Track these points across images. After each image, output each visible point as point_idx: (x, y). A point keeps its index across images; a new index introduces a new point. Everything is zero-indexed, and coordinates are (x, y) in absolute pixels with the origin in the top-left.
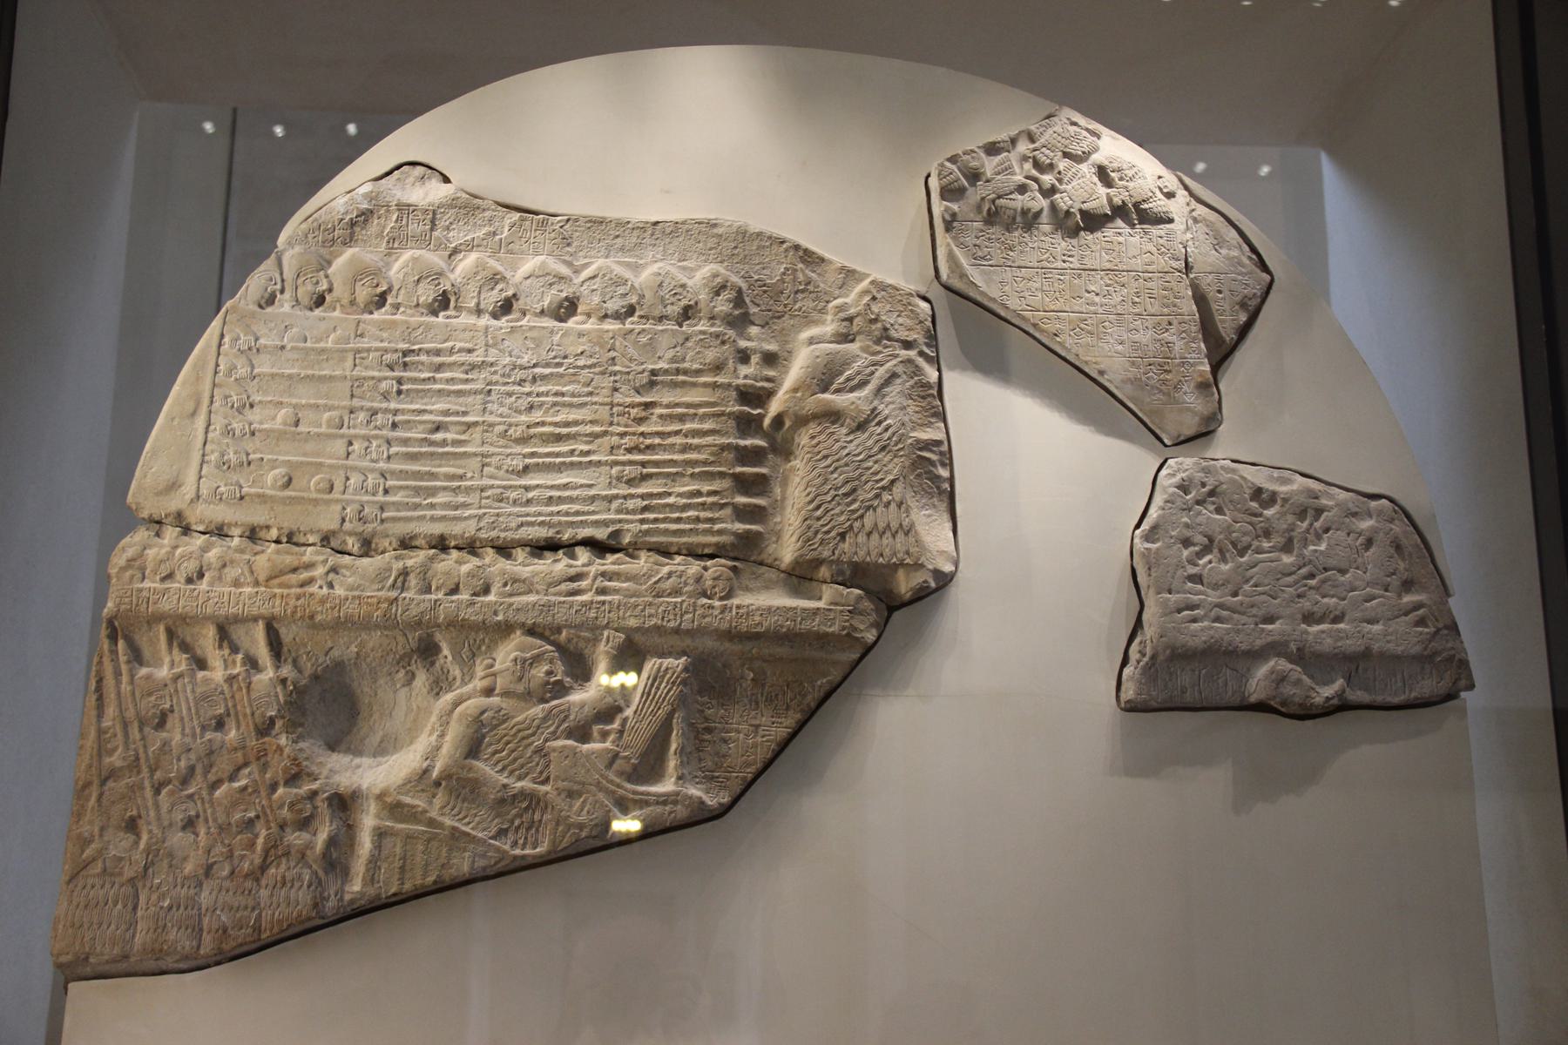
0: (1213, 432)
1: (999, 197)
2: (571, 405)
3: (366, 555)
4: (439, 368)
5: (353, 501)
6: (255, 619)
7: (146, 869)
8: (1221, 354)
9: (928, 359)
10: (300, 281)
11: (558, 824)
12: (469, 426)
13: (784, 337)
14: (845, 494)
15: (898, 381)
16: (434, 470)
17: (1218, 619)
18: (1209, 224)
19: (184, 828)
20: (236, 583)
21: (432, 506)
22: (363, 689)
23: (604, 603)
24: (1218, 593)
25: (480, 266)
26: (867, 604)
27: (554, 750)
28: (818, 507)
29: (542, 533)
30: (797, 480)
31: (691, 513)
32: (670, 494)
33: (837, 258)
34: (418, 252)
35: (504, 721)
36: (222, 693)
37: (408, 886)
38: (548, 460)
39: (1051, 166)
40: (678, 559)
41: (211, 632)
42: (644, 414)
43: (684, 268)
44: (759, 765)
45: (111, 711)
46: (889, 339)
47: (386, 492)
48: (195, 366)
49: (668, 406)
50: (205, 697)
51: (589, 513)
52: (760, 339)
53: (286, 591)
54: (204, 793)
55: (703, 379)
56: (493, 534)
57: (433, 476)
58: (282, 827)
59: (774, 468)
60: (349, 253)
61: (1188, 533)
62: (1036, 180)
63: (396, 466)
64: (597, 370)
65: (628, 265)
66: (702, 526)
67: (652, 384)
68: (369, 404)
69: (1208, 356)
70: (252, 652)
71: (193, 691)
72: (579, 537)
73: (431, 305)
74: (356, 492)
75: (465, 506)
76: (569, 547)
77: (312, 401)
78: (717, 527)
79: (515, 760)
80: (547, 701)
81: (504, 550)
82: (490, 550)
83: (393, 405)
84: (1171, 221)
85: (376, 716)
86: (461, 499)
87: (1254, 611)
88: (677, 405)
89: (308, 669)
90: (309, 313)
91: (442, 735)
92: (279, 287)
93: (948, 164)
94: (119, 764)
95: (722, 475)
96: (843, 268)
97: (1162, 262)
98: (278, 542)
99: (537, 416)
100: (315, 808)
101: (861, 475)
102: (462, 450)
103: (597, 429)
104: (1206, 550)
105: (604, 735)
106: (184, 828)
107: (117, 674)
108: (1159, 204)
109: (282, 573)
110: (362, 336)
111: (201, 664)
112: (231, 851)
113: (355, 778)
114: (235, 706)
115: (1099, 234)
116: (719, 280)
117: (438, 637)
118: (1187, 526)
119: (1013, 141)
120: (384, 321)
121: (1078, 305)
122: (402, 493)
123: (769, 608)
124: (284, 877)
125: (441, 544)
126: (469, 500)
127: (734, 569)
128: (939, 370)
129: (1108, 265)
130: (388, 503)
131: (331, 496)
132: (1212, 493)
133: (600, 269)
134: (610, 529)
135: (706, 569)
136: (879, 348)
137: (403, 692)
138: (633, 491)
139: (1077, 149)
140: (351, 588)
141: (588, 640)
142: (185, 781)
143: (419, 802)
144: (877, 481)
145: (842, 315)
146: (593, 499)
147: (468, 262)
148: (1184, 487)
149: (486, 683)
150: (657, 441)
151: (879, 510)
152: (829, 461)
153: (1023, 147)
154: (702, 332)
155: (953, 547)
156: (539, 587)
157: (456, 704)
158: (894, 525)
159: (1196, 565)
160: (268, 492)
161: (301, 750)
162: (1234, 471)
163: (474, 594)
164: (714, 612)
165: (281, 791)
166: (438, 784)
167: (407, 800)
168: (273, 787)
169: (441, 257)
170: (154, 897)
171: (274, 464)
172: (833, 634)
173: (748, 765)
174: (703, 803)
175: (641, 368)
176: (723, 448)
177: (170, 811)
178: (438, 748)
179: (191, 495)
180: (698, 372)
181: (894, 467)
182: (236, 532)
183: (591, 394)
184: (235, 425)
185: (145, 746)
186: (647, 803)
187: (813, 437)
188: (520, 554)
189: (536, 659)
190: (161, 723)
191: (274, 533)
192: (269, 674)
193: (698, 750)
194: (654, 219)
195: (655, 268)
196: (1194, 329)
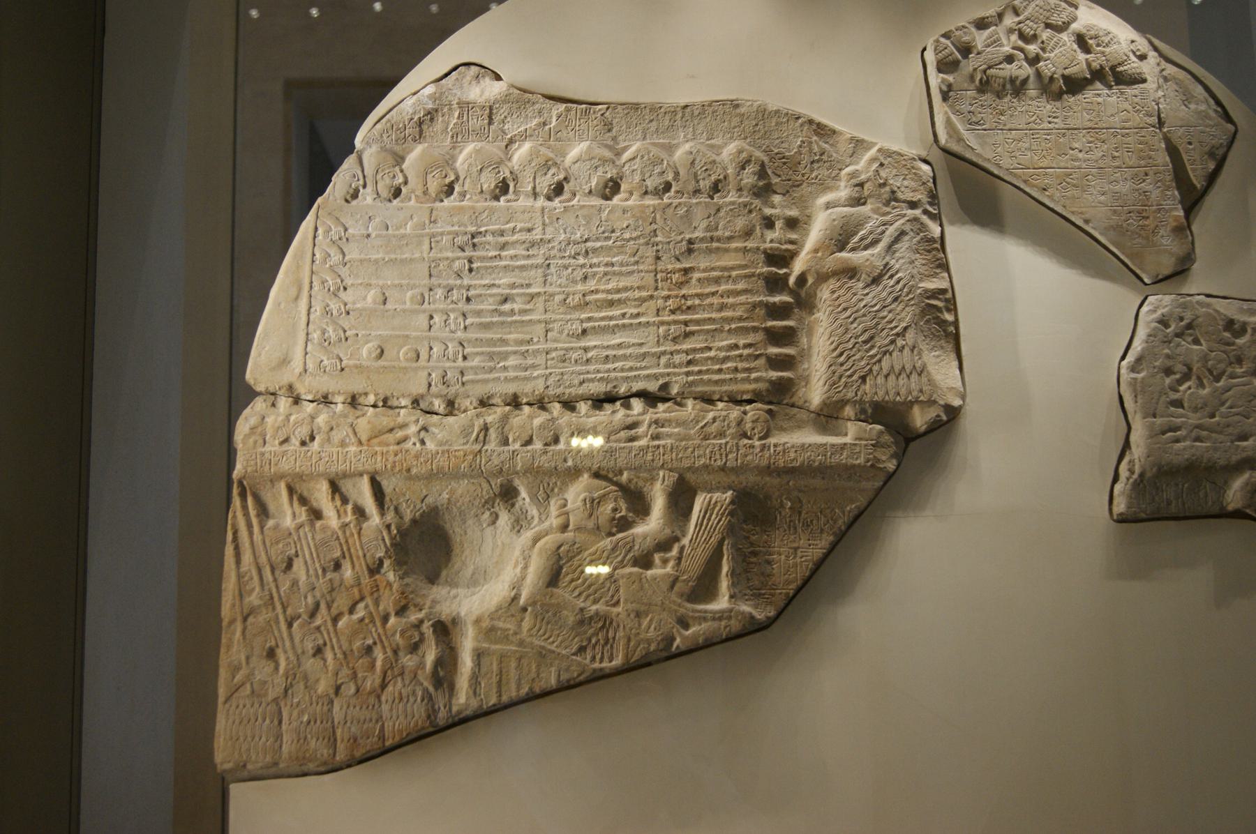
0: (1188, 269)
1: (990, 68)
2: (620, 274)
3: (450, 414)
4: (504, 246)
6: (361, 475)
7: (286, 691)
8: (1192, 200)
9: (932, 217)
10: (379, 177)
11: (629, 640)
13: (803, 203)
14: (864, 342)
15: (907, 238)
16: (505, 337)
17: (1198, 439)
18: (1178, 82)
19: (314, 655)
20: (343, 444)
21: (505, 368)
22: (455, 530)
23: (658, 447)
24: (1198, 415)
25: (534, 153)
26: (887, 438)
27: (623, 577)
28: (841, 354)
29: (598, 388)
30: (821, 330)
31: (729, 365)
32: (710, 349)
33: (846, 129)
34: (479, 145)
35: (579, 553)
36: (338, 538)
37: (505, 699)
38: (603, 323)
39: (1035, 37)
40: (720, 405)
41: (324, 487)
43: (712, 146)
44: (799, 582)
45: (247, 557)
46: (896, 200)
47: (465, 358)
48: (295, 256)
49: (705, 271)
50: (324, 543)
51: (641, 368)
52: (783, 207)
53: (385, 449)
54: (329, 623)
55: (734, 245)
56: (559, 391)
57: (504, 342)
58: (395, 652)
59: (800, 320)
60: (419, 149)
61: (1169, 363)
62: (1022, 50)
63: (472, 335)
64: (642, 241)
65: (662, 146)
66: (740, 376)
67: (690, 251)
68: (445, 283)
69: (1181, 202)
70: (360, 502)
71: (313, 538)
73: (493, 191)
74: (438, 360)
75: (534, 367)
76: (626, 400)
77: (396, 282)
78: (753, 375)
80: (614, 535)
81: (569, 405)
82: (557, 405)
83: (466, 282)
84: (1144, 81)
85: (467, 552)
86: (530, 361)
87: (1230, 430)
88: (713, 269)
89: (408, 516)
90: (389, 204)
91: (526, 567)
92: (361, 182)
93: (942, 40)
94: (257, 602)
95: (755, 329)
96: (852, 139)
97: (1137, 119)
98: (375, 406)
99: (592, 284)
100: (422, 634)
101: (877, 324)
102: (528, 318)
103: (644, 294)
104: (1186, 377)
105: (665, 562)
106: (314, 655)
107: (250, 526)
108: (1133, 65)
109: (381, 433)
110: (435, 222)
111: (316, 514)
114: (349, 549)
115: (1080, 97)
116: (744, 155)
117: (517, 482)
118: (1168, 357)
119: (1000, 16)
120: (454, 208)
121: (1063, 161)
122: (477, 359)
123: (803, 445)
124: (400, 694)
125: (515, 402)
127: (770, 412)
128: (941, 225)
129: (1090, 124)
130: (467, 368)
132: (1189, 326)
133: (638, 151)
134: (661, 382)
135: (745, 413)
136: (888, 209)
138: (678, 347)
139: (1057, 20)
140: (441, 444)
141: (646, 480)
142: (313, 614)
143: (510, 626)
144: (892, 329)
145: (854, 181)
146: (644, 355)
147: (522, 151)
148: (1163, 322)
149: (560, 521)
150: (697, 302)
151: (894, 354)
152: (848, 313)
153: (1009, 21)
154: (733, 203)
155: (960, 383)
157: (536, 540)
158: (908, 367)
159: (1178, 391)
161: (407, 585)
162: (1208, 305)
163: (546, 444)
164: (754, 452)
166: (524, 610)
167: (501, 624)
168: (385, 619)
169: (499, 148)
170: (295, 713)
173: (788, 582)
174: (752, 617)
175: (679, 238)
176: (755, 306)
178: (523, 578)
179: (299, 369)
180: (730, 238)
181: (907, 315)
182: (339, 399)
183: (637, 263)
184: (332, 306)
185: (277, 587)
186: (705, 619)
187: (833, 292)
188: (583, 407)
189: (602, 498)
190: (289, 565)
191: (371, 399)
192: (375, 519)
193: (746, 571)
194: (683, 102)
195: (687, 147)
196: (1169, 178)
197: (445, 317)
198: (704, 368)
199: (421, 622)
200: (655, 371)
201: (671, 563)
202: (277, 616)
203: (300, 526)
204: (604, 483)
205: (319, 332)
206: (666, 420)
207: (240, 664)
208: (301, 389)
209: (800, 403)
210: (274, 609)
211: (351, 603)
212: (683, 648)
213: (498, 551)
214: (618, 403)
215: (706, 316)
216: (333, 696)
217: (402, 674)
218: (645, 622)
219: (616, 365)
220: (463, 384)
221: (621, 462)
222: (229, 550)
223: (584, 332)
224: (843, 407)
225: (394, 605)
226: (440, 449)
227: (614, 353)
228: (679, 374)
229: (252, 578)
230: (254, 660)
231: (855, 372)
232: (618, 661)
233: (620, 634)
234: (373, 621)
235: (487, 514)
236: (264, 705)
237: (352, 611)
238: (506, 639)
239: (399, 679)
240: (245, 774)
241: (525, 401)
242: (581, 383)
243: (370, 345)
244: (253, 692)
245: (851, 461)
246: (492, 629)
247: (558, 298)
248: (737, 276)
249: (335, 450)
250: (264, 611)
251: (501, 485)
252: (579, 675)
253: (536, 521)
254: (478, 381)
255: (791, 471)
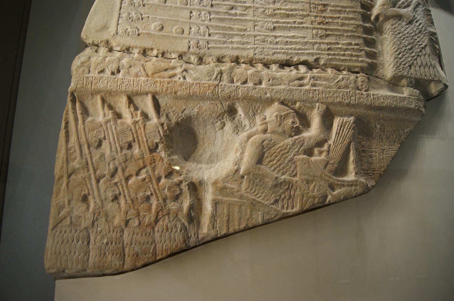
5: (194, 38)
6: (147, 94)
7: (93, 223)
12: (247, 8)
15: (421, 6)
16: (232, 26)
20: (137, 75)
21: (232, 42)
22: (200, 131)
23: (315, 90)
26: (421, 97)
27: (299, 160)
31: (348, 52)
35: (274, 146)
37: (231, 230)
38: (284, 25)
40: (345, 72)
41: (124, 100)
42: (323, 9)
45: (73, 138)
47: (210, 35)
49: (333, 6)
50: (123, 132)
51: (305, 49)
53: (162, 80)
54: (123, 181)
56: (262, 57)
58: (164, 200)
59: (377, 37)
63: (213, 23)
66: (354, 58)
70: (145, 110)
71: (116, 129)
72: (301, 60)
75: (248, 43)
76: (296, 66)
79: (280, 165)
80: (292, 137)
81: (267, 65)
82: (260, 65)
85: (206, 144)
86: (245, 40)
88: (337, 6)
89: (174, 120)
91: (243, 153)
94: (77, 166)
98: (157, 56)
100: (181, 190)
102: (244, 18)
103: (305, 13)
105: (321, 153)
106: (113, 201)
107: (76, 120)
109: (160, 71)
111: (118, 116)
112: (138, 212)
113: (200, 174)
114: (138, 137)
123: (386, 96)
124: (167, 226)
125: (237, 60)
126: (249, 41)
127: (368, 78)
130: (211, 40)
131: (183, 36)
134: (315, 57)
135: (357, 77)
137: (219, 133)
140: (195, 79)
142: (113, 175)
143: (235, 186)
146: (306, 43)
149: (263, 127)
150: (331, 21)
151: (422, 57)
152: (400, 35)
156: (285, 82)
157: (249, 137)
158: (429, 64)
160: (152, 32)
161: (172, 160)
163: (255, 84)
165: (163, 181)
166: (243, 177)
167: (229, 185)
168: (159, 179)
170: (99, 238)
171: (155, 20)
172: (412, 108)
176: (358, 26)
177: (105, 191)
178: (241, 159)
182: (136, 51)
185: (91, 157)
186: (344, 186)
187: (392, 25)
188: (274, 67)
189: (286, 116)
190: (100, 144)
191: (155, 52)
192: (154, 120)
197: (199, 13)
198: (336, 53)
199: (181, 182)
200: (312, 51)
201: (324, 154)
202: (90, 175)
203: (107, 122)
204: (287, 108)
205: (126, 14)
206: (318, 77)
207: (64, 205)
208: (113, 43)
209: (381, 76)
210: (88, 171)
211: (137, 169)
212: (332, 202)
213: (224, 144)
214: (292, 68)
215: (337, 28)
216: (124, 227)
217: (168, 214)
218: (312, 187)
219: (292, 46)
220: (208, 48)
221: (296, 97)
222: (62, 133)
223: (274, 28)
224: (401, 80)
225: (165, 171)
226: (195, 82)
227: (290, 40)
228: (324, 54)
229: (75, 151)
230: (73, 202)
231: (406, 63)
232: (297, 209)
233: (298, 192)
234: (151, 181)
235: (219, 123)
236: (78, 231)
237: (137, 174)
238: (232, 194)
239: (167, 217)
240: (65, 275)
241: (242, 61)
242: (274, 54)
243: (156, 23)
244: (71, 223)
245: (408, 106)
246: (224, 188)
247: (260, 10)
248: (349, 11)
249: (132, 78)
250: (82, 172)
251: (229, 106)
252: (275, 217)
253: (247, 127)
254: (217, 48)
255: (380, 108)
